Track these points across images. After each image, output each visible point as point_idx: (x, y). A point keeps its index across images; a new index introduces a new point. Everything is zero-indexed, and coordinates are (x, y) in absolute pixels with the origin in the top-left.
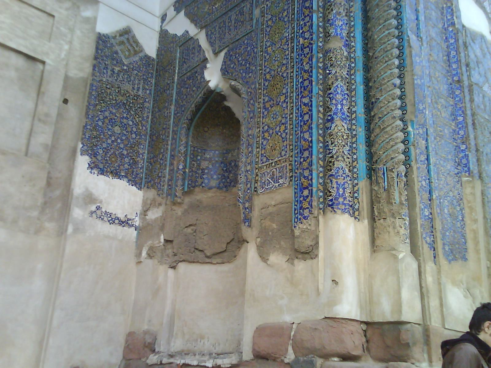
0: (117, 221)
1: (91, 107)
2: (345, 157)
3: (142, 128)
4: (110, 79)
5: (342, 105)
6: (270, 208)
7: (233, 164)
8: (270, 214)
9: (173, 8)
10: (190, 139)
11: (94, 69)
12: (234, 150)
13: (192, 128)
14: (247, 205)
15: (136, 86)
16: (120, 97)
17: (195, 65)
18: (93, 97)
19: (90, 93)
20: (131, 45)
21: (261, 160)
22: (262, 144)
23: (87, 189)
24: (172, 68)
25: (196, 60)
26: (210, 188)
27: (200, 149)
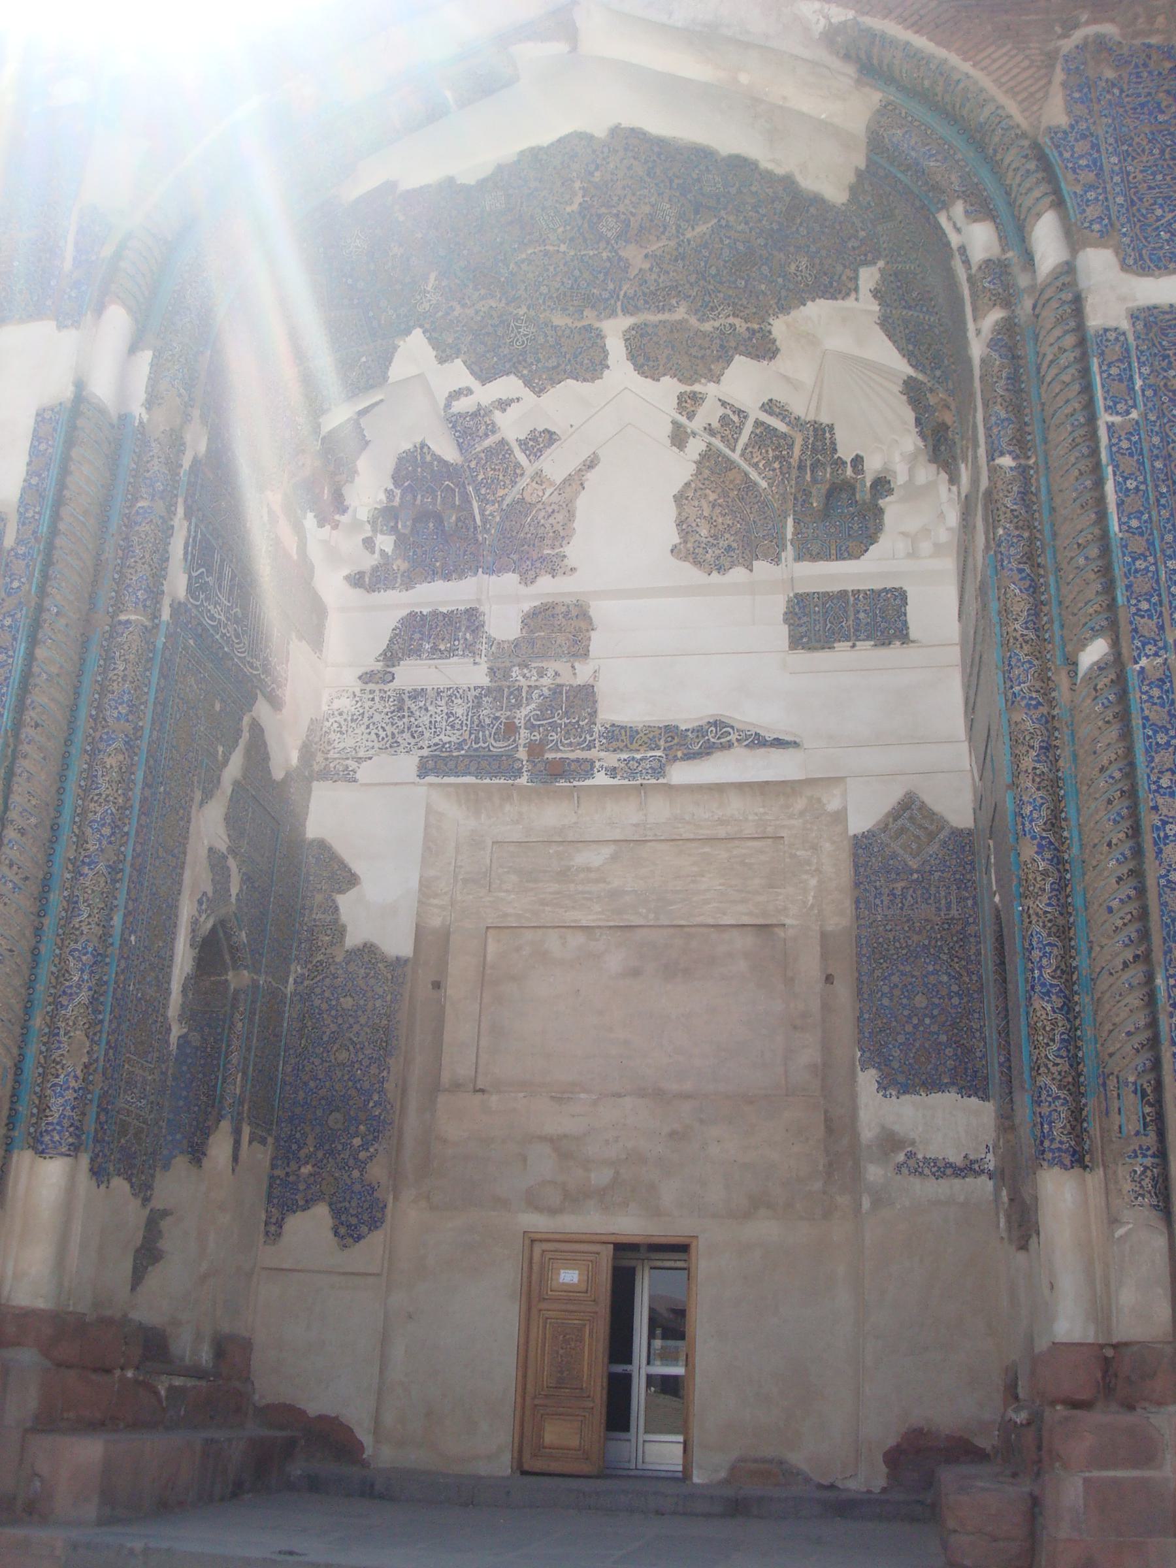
0: (949, 1171)
1: (865, 979)
2: (1050, 1065)
3: (971, 980)
4: (891, 912)
5: (1041, 968)
11: (857, 908)
15: (943, 902)
16: (916, 938)
18: (864, 959)
19: (859, 955)
20: (920, 827)
23: (883, 1127)
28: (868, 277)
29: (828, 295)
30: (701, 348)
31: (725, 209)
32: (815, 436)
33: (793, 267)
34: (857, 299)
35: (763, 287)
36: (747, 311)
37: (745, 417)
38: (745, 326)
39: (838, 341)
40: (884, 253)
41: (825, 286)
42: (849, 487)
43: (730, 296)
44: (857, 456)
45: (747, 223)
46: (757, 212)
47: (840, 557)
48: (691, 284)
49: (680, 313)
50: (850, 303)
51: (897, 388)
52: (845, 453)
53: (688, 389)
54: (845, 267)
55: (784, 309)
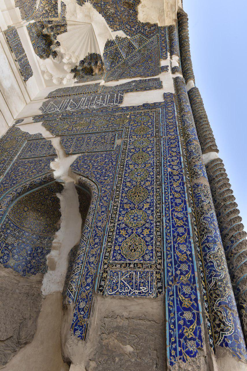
6: (119, 320)
7: (39, 251)
8: (118, 328)
9: (32, 118)
10: (9, 210)
12: (44, 239)
13: (15, 202)
14: (82, 305)
17: (42, 156)
21: (114, 256)
22: (116, 239)
24: (14, 151)
25: (44, 152)
26: (6, 267)
27: (12, 223)
28: (121, 34)
33: (109, 7)
34: (112, 31)
40: (133, 37)
41: (109, 20)
42: (50, 43)
44: (59, 43)
47: (33, 46)
50: (110, 30)
51: (89, 51)
54: (119, 25)
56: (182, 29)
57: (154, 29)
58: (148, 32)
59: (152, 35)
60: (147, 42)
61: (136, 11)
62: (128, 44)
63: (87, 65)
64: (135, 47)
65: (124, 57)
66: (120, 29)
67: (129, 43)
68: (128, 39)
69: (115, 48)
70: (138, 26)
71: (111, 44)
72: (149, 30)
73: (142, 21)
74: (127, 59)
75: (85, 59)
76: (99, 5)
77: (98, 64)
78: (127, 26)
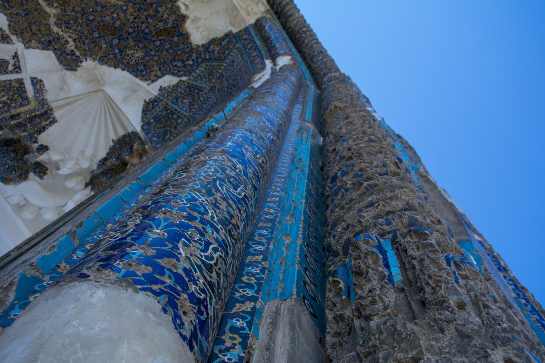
28: (169, 81)
29: (135, 74)
30: (40, 30)
31: (134, 4)
32: (42, 115)
33: (132, 52)
34: (148, 84)
35: (104, 46)
36: (82, 45)
37: (17, 72)
38: (73, 48)
39: (115, 93)
41: (138, 70)
43: (83, 33)
45: (135, 18)
46: (147, 19)
48: (73, 10)
49: (52, 11)
50: (144, 84)
51: (113, 136)
52: (43, 138)
53: (8, 32)
54: (160, 69)
55: (103, 60)
56: (286, 18)
57: (228, 42)
58: (218, 53)
59: (227, 52)
60: (223, 68)
61: (184, 34)
62: (188, 90)
63: (115, 162)
64: (201, 87)
65: (185, 114)
66: (164, 75)
67: (188, 86)
68: (184, 81)
69: (161, 107)
70: (197, 54)
71: (153, 105)
72: (218, 49)
73: (200, 44)
74: (191, 114)
75: (108, 154)
76: (111, 56)
77: (135, 147)
78: (175, 64)
